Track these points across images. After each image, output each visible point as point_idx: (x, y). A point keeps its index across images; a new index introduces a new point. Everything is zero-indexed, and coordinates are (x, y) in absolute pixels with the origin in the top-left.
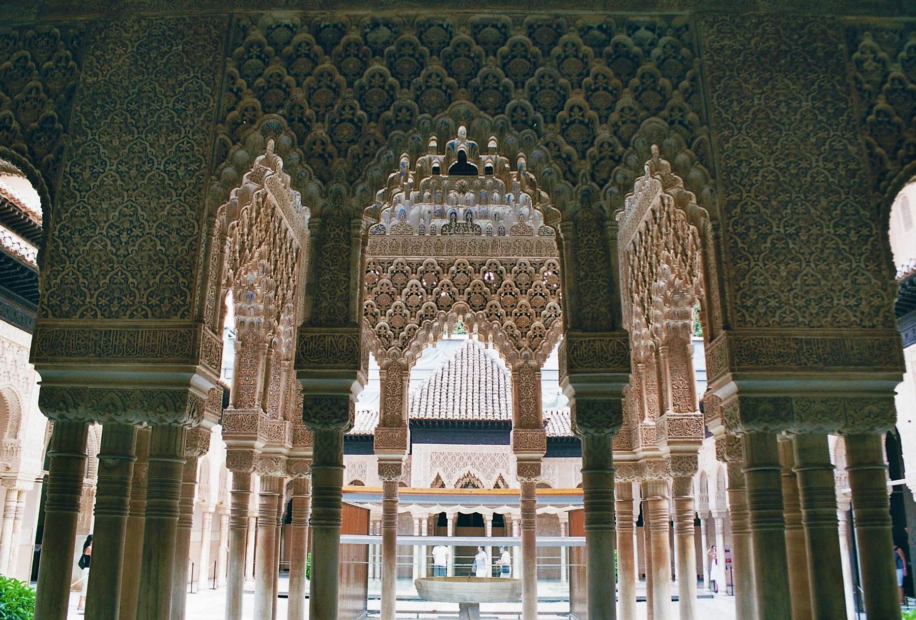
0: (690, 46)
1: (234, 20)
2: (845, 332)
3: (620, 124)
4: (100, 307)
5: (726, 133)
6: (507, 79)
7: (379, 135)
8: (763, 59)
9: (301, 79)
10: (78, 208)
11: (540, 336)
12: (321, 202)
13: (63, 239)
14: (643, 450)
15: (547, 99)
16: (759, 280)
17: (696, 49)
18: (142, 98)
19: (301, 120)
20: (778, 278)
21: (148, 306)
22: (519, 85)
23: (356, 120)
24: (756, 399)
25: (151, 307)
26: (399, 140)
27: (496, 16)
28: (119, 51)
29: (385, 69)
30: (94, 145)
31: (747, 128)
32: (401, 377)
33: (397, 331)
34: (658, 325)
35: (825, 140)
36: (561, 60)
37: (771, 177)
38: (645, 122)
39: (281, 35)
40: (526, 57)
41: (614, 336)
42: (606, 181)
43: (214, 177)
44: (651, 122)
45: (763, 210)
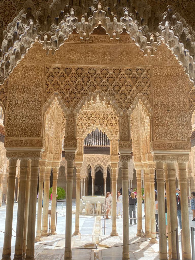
1: (45, 66)
4: (20, 135)
6: (108, 84)
8: (166, 78)
9: (62, 82)
10: (12, 112)
11: (118, 131)
12: (68, 112)
13: (9, 119)
14: (143, 162)
16: (160, 130)
17: (151, 76)
19: (63, 92)
20: (164, 130)
21: (31, 134)
23: (75, 93)
24: (158, 155)
26: (84, 98)
27: (106, 67)
28: (18, 73)
30: (15, 97)
31: (161, 95)
34: (147, 131)
35: (179, 98)
38: (138, 94)
39: (57, 70)
40: (112, 77)
41: (129, 142)
42: (129, 108)
43: (44, 106)
44: (140, 94)
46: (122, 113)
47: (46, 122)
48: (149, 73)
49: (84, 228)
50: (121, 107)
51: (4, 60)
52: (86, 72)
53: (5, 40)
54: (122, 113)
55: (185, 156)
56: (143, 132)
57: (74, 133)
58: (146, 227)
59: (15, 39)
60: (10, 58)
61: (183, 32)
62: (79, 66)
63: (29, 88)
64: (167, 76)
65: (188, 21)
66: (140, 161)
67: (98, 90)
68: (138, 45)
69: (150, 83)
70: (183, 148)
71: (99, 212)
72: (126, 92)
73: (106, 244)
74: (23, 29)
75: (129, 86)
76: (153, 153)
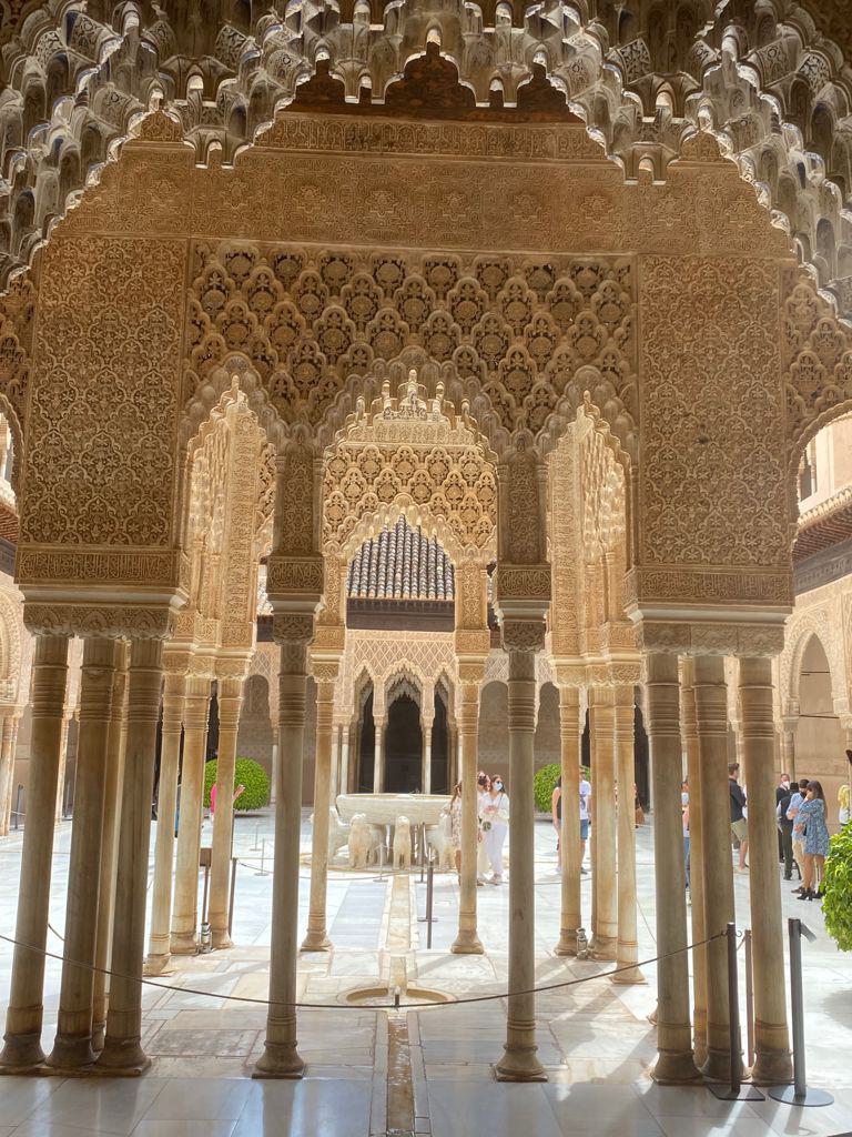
0: (629, 290)
1: (192, 246)
2: (743, 569)
3: (556, 371)
5: (653, 382)
6: (455, 324)
7: (337, 377)
8: (697, 305)
11: (487, 532)
13: (38, 466)
14: (589, 656)
15: (492, 346)
16: (669, 521)
18: (105, 326)
19: (263, 358)
21: (128, 533)
22: (466, 330)
23: (316, 361)
24: (658, 625)
25: (131, 534)
26: (356, 383)
27: (448, 255)
29: (343, 309)
30: (61, 373)
32: (339, 572)
33: (335, 523)
34: (606, 530)
36: (507, 303)
37: (691, 425)
39: (240, 265)
40: (472, 300)
43: (184, 412)
45: (678, 457)
46: (509, 450)
47: (194, 487)
48: (627, 283)
49: (346, 921)
50: (508, 422)
51: (9, 181)
52: (365, 273)
53: (11, 86)
54: (509, 450)
55: (770, 629)
56: (590, 537)
57: (311, 530)
58: (595, 918)
59: (59, 92)
60: (38, 181)
61: (798, 76)
62: (333, 250)
63: (120, 336)
64: (699, 298)
65: (823, 22)
66: (577, 652)
67: (414, 349)
68: (597, 136)
69: (629, 325)
70: (759, 597)
71: (402, 860)
72: (530, 360)
73: (436, 986)
74: (94, 43)
75: (541, 338)
76: (636, 615)
